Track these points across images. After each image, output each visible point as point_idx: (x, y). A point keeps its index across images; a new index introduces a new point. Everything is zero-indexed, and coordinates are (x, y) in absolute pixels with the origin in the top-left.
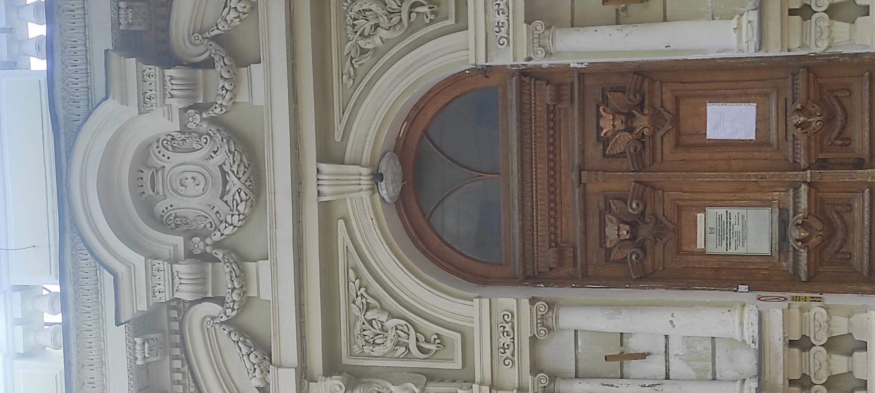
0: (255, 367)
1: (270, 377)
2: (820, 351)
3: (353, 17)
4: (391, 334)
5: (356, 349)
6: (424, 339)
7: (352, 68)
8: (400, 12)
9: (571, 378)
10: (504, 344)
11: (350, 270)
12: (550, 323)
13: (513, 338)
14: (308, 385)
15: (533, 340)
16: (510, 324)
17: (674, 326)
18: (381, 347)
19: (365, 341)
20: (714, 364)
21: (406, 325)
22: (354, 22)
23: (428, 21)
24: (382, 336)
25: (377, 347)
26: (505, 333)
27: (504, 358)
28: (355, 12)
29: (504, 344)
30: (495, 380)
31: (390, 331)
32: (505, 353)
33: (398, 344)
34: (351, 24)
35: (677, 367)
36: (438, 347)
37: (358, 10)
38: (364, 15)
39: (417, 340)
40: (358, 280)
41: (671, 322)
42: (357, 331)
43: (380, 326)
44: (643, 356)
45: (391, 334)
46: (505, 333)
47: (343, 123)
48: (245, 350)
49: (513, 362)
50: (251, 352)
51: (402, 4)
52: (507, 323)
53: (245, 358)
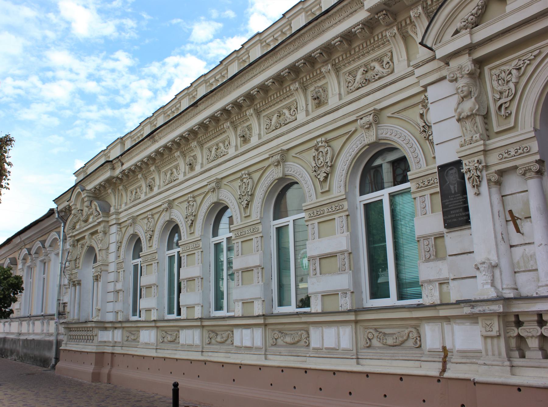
0: (466, 21)
1: (463, 32)
2: (538, 332)
4: (505, 87)
5: (493, 72)
6: (507, 106)
9: (500, 193)
10: (510, 151)
11: (539, 50)
12: (528, 175)
13: (514, 156)
14: (466, 54)
15: (515, 168)
16: (523, 152)
17: (539, 246)
18: (497, 84)
19: (499, 75)
20: (524, 271)
21: (512, 94)
24: (503, 82)
25: (496, 82)
26: (516, 151)
27: (503, 154)
29: (510, 151)
30: (490, 152)
31: (507, 86)
32: (505, 153)
33: (501, 93)
35: (518, 252)
36: (504, 115)
39: (505, 103)
40: (533, 57)
41: (541, 244)
42: (503, 68)
43: (509, 80)
44: (518, 231)
45: (505, 87)
46: (516, 151)
48: (474, 12)
49: (501, 159)
50: (474, 16)
52: (523, 150)
53: (470, 14)
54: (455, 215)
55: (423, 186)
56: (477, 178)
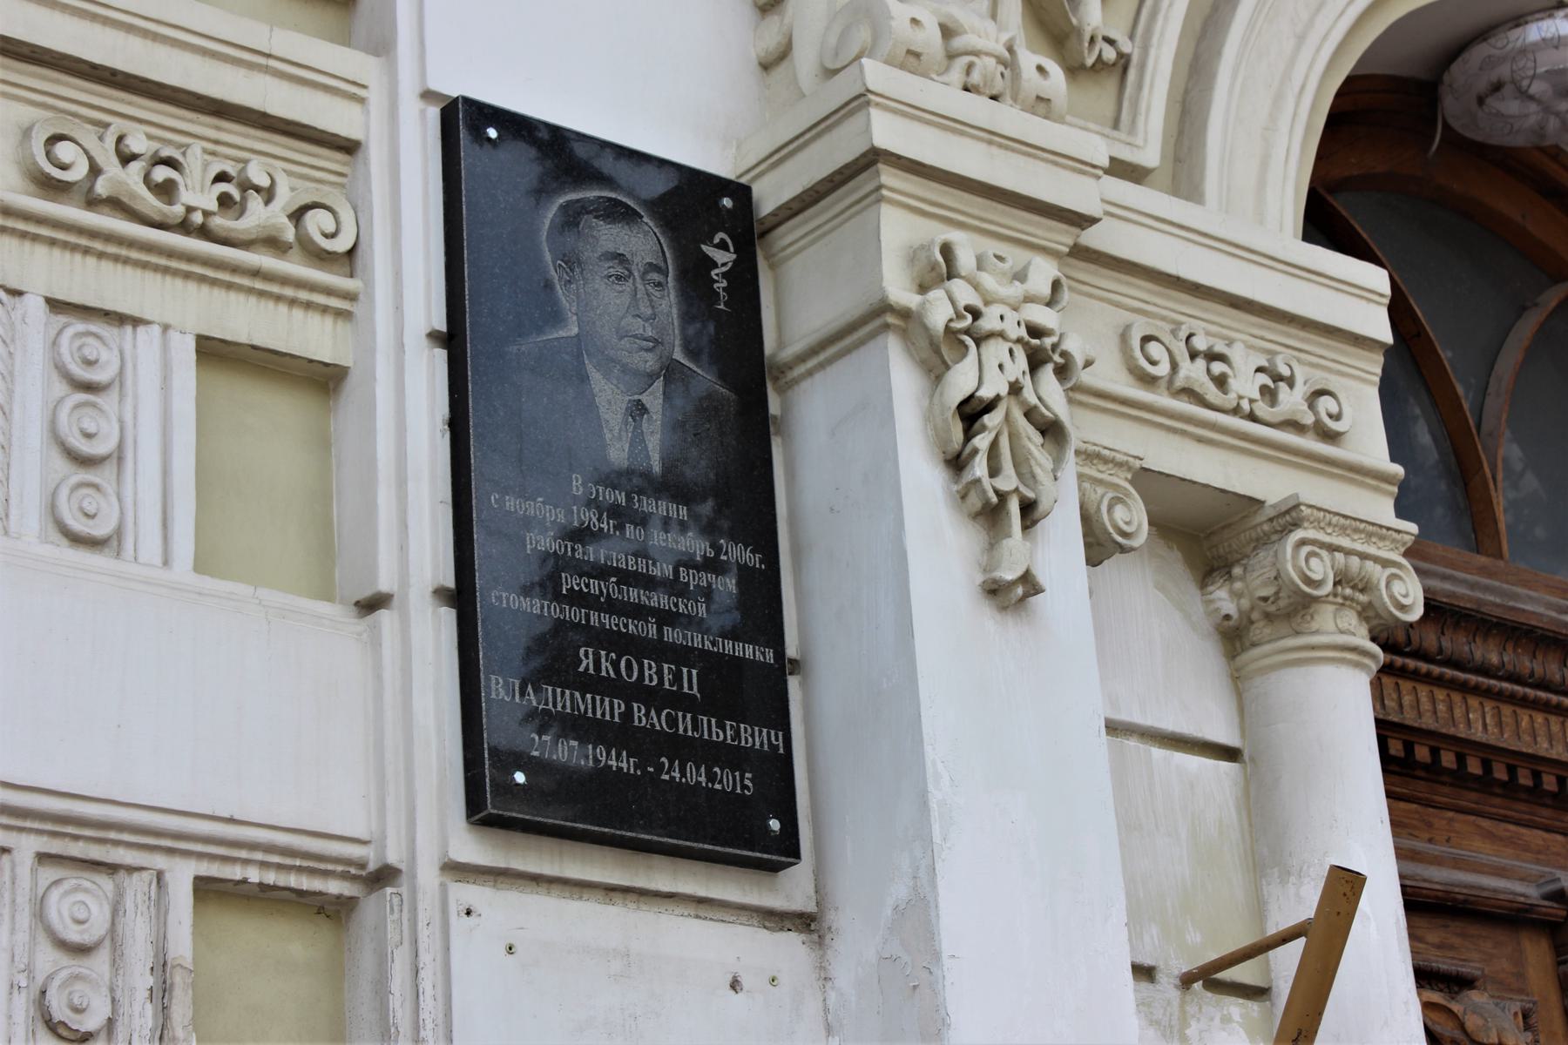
54: (619, 706)
55: (151, 203)
56: (1032, 438)
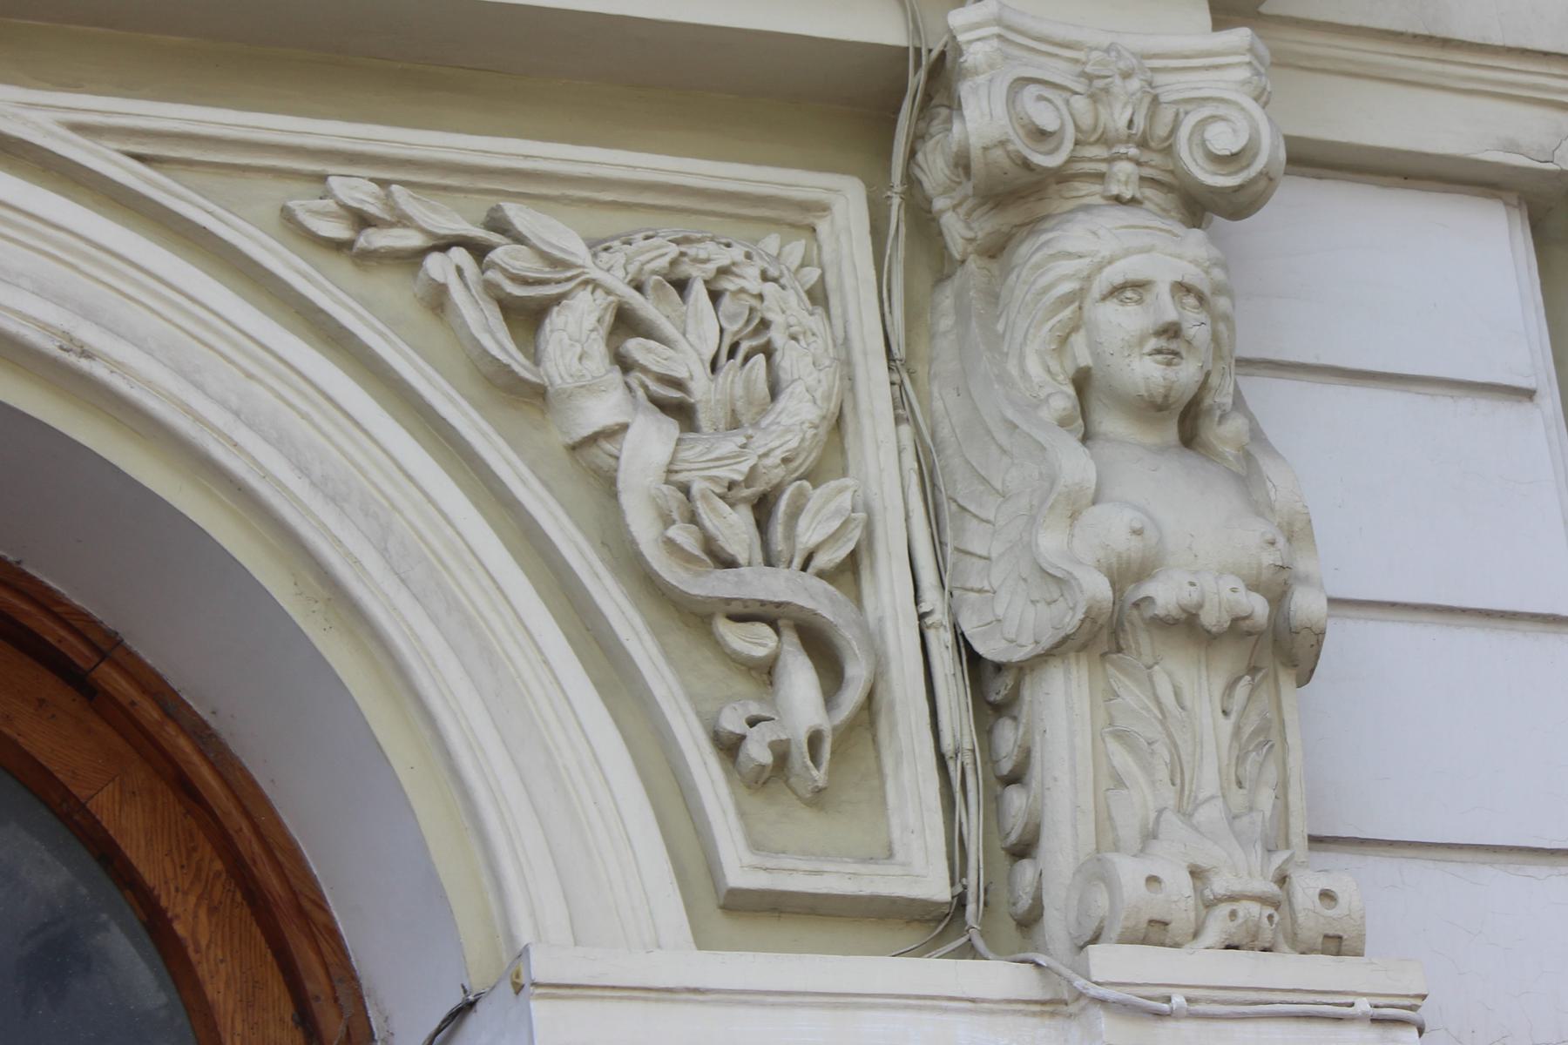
3: (729, 284)
7: (414, 240)
8: (769, 561)
22: (699, 292)
23: (732, 722)
28: (761, 297)
34: (687, 269)
37: (770, 316)
38: (745, 347)
47: (64, 140)
51: (821, 574)
